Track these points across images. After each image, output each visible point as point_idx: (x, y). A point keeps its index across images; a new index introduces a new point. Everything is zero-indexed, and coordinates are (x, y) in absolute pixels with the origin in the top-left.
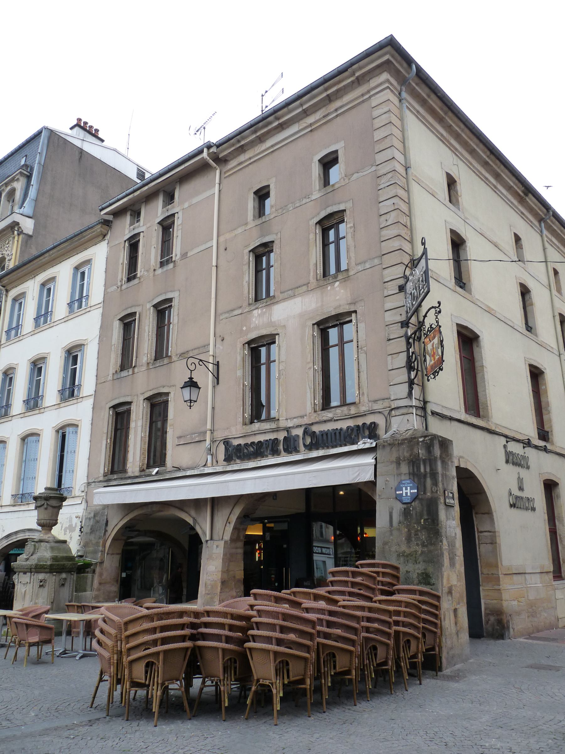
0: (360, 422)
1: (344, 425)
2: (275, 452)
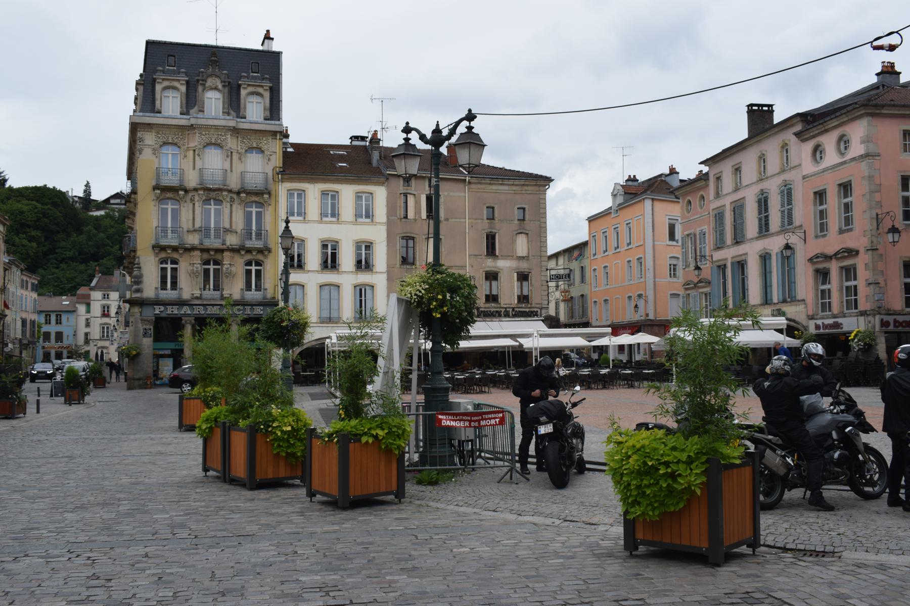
0: (532, 310)
1: (527, 310)
2: (500, 315)
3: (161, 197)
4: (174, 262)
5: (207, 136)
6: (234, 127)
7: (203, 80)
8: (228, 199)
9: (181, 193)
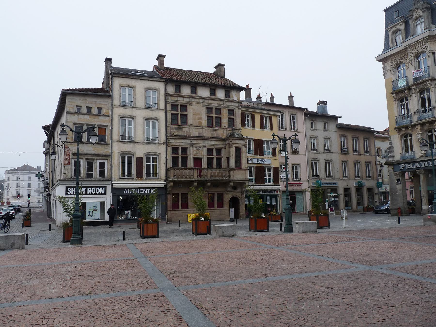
3: (398, 98)
4: (410, 135)
5: (415, 50)
6: (429, 36)
7: (410, 16)
8: (433, 86)
9: (406, 91)
